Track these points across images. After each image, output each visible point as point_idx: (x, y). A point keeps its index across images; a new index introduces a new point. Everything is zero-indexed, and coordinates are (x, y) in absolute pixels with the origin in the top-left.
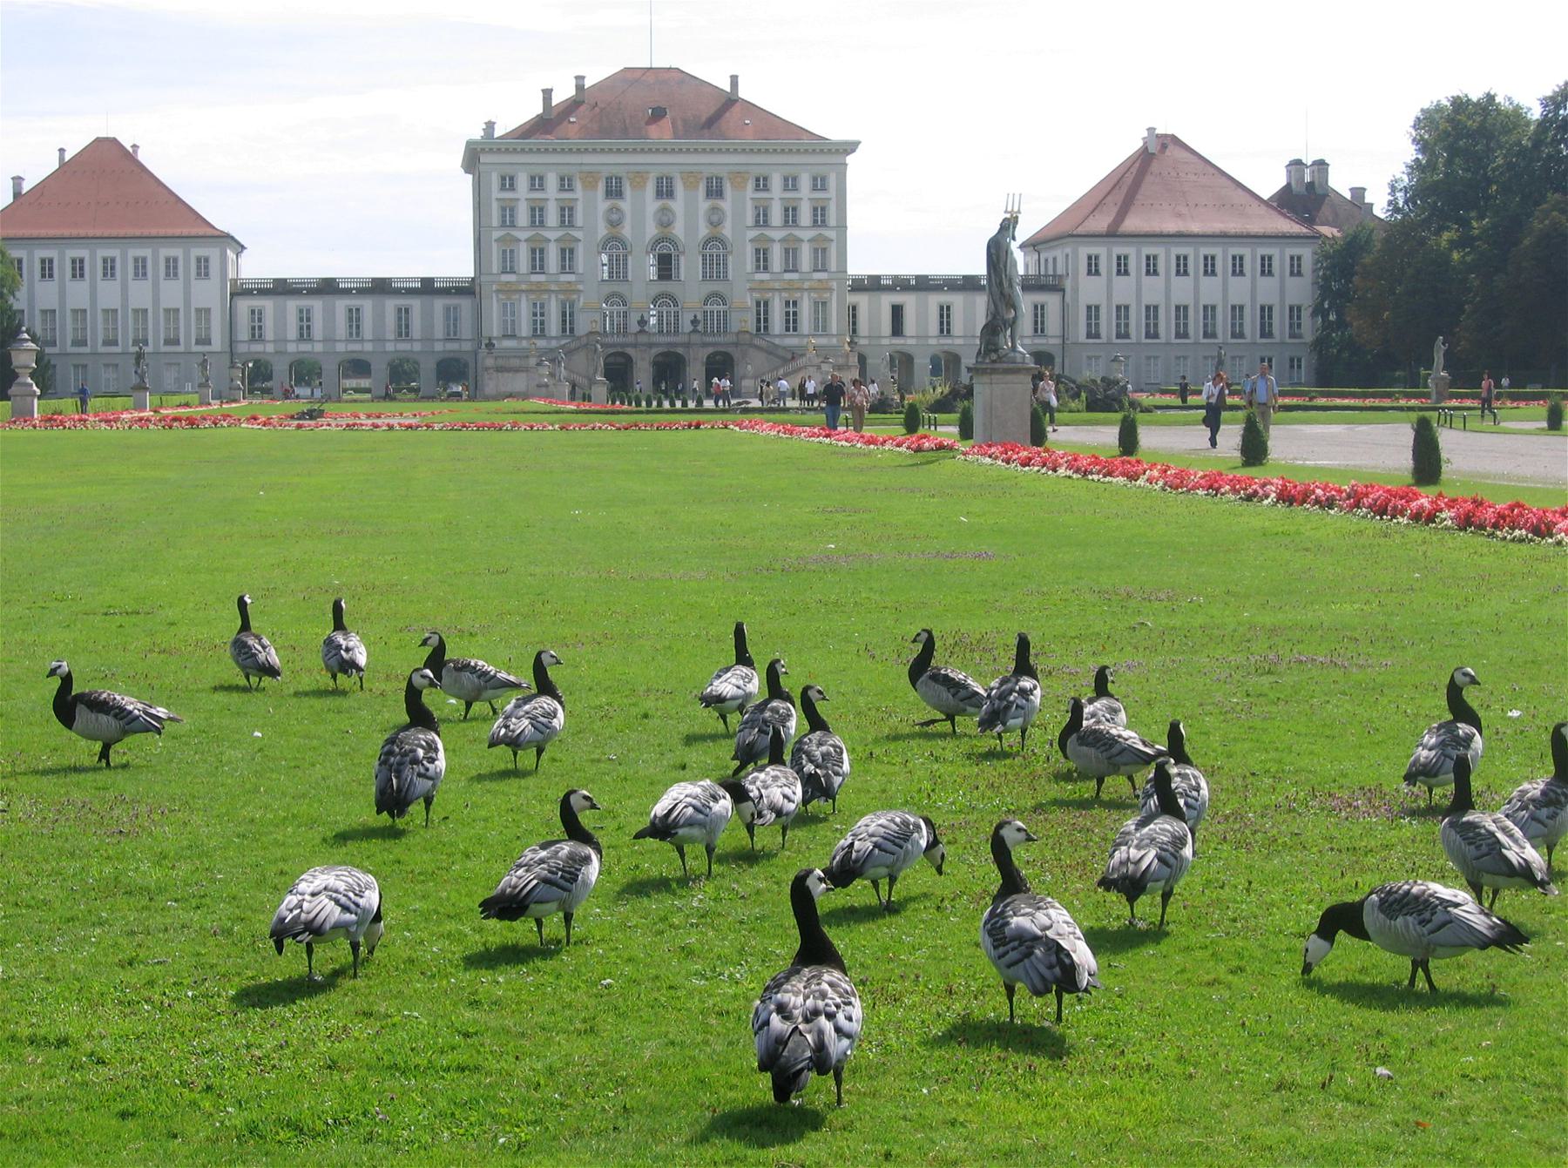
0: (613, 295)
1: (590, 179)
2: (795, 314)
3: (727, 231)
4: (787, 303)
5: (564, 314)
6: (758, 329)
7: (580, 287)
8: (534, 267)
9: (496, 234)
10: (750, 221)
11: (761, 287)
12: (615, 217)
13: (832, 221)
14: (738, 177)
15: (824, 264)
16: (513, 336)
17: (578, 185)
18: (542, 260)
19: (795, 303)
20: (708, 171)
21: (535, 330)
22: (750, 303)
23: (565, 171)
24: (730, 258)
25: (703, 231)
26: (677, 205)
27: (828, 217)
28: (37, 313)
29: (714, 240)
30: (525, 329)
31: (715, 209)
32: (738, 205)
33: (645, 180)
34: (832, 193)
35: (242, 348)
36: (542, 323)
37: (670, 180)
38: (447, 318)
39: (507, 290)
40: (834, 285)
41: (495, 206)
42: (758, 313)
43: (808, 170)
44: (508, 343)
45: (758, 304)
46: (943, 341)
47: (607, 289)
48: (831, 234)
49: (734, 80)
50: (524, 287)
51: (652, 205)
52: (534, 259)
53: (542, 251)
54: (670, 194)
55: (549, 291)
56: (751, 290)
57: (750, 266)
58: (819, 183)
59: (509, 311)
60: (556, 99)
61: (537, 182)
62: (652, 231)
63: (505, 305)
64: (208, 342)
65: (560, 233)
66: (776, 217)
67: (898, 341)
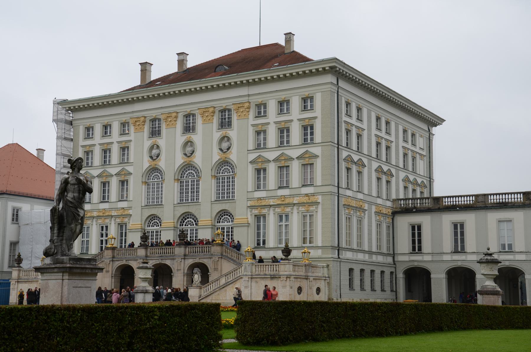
1: (139, 123)
3: (233, 156)
4: (281, 217)
7: (130, 212)
22: (251, 220)
23: (124, 118)
26: (197, 138)
29: (225, 163)
32: (242, 131)
34: (318, 112)
40: (319, 199)
47: (148, 212)
56: (252, 207)
57: (251, 184)
58: (307, 102)
67: (456, 257)
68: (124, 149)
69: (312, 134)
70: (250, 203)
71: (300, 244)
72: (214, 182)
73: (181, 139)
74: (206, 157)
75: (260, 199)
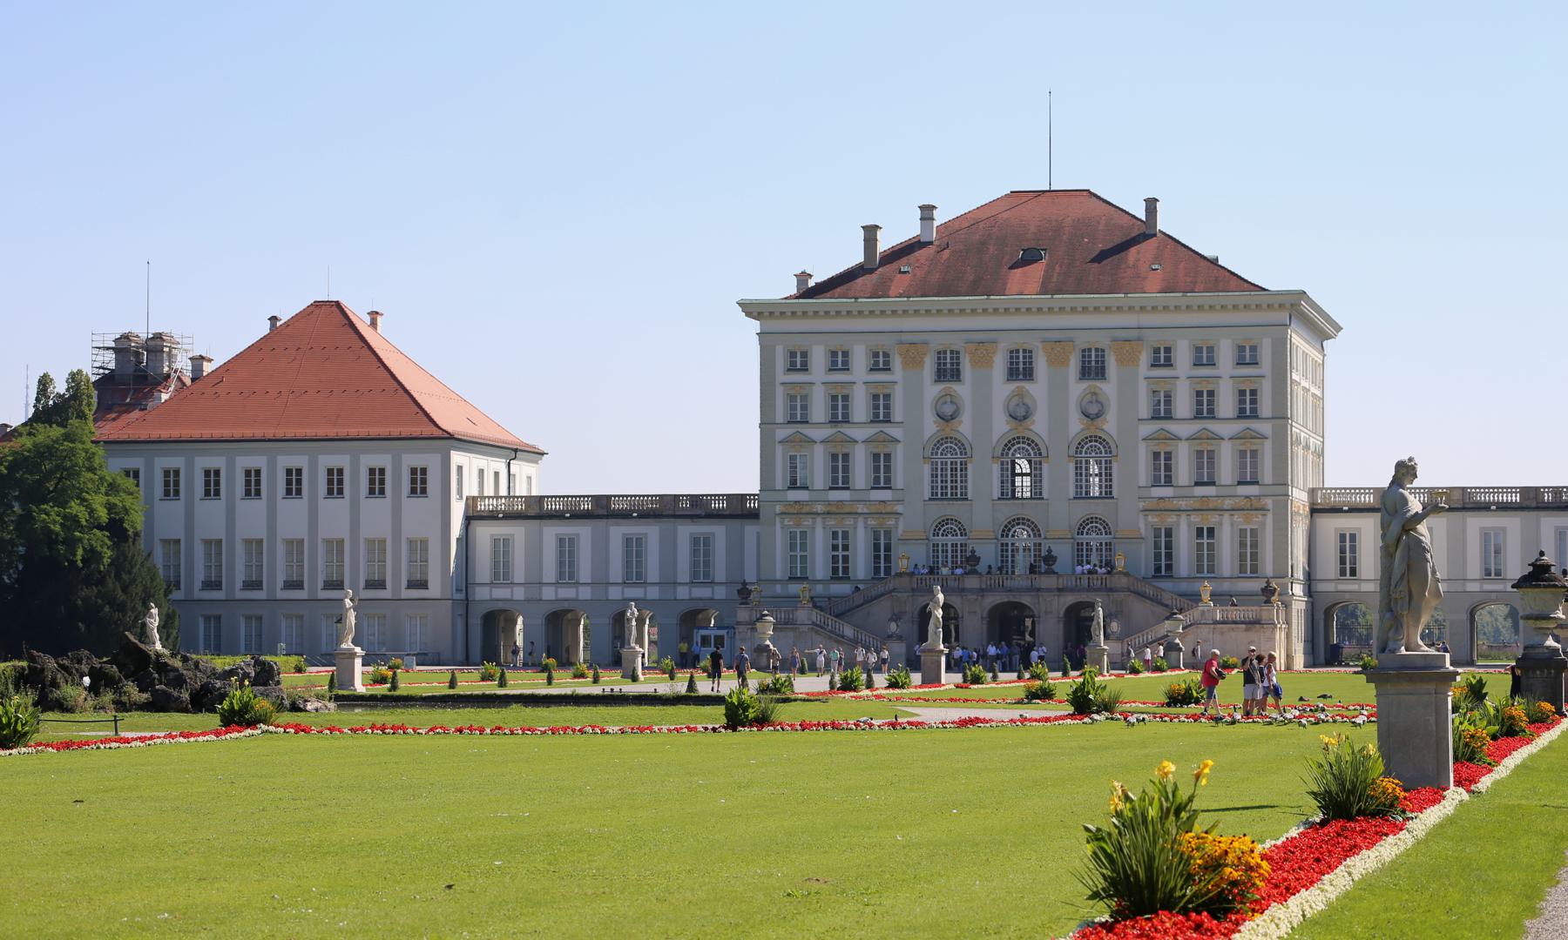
0: (946, 521)
2: (1211, 547)
4: (1200, 532)
5: (876, 547)
6: (1158, 569)
7: (899, 508)
8: (835, 480)
9: (782, 433)
10: (1144, 411)
11: (1161, 507)
12: (948, 410)
13: (1266, 408)
14: (1128, 343)
15: (1254, 474)
16: (804, 579)
17: (897, 363)
18: (846, 469)
19: (1211, 531)
20: (1083, 341)
21: (835, 570)
24: (1115, 465)
25: (1076, 425)
26: (1037, 390)
27: (1261, 406)
28: (279, 541)
30: (820, 567)
34: (1266, 367)
35: (481, 594)
36: (846, 559)
37: (1028, 353)
38: (695, 552)
39: (798, 511)
40: (1269, 502)
41: (780, 393)
42: (1157, 546)
43: (1246, 338)
44: (794, 588)
45: (1157, 532)
46: (1488, 587)
49: (1151, 204)
50: (819, 508)
51: (1002, 390)
52: (835, 469)
53: (846, 457)
54: (1028, 374)
57: (1143, 473)
59: (798, 542)
60: (884, 244)
61: (839, 361)
62: (1001, 426)
63: (793, 536)
64: (423, 585)
65: (871, 431)
66: (1183, 404)
69: (1254, 401)
70: (1141, 505)
71: (1236, 573)
72: (1072, 466)
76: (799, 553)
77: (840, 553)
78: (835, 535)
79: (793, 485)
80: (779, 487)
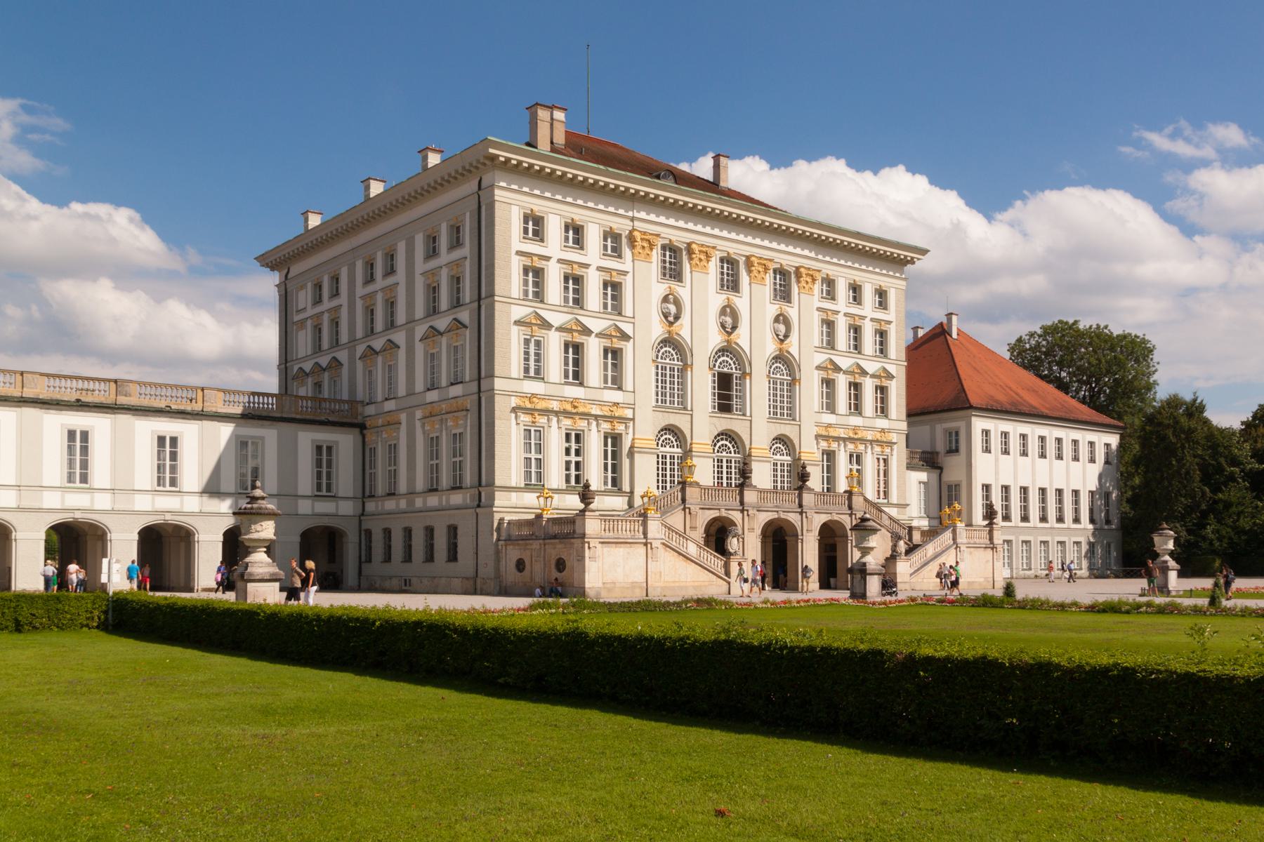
9: (519, 312)
17: (627, 252)
21: (568, 481)
25: (771, 348)
31: (781, 318)
33: (708, 257)
34: (891, 315)
40: (894, 437)
41: (516, 265)
48: (892, 369)
50: (555, 405)
51: (717, 300)
55: (586, 416)
56: (818, 437)
59: (534, 441)
62: (716, 339)
68: (613, 288)
73: (717, 300)
74: (757, 342)
75: (830, 426)
76: (533, 456)
77: (573, 458)
78: (568, 436)
79: (527, 376)
80: (515, 375)
